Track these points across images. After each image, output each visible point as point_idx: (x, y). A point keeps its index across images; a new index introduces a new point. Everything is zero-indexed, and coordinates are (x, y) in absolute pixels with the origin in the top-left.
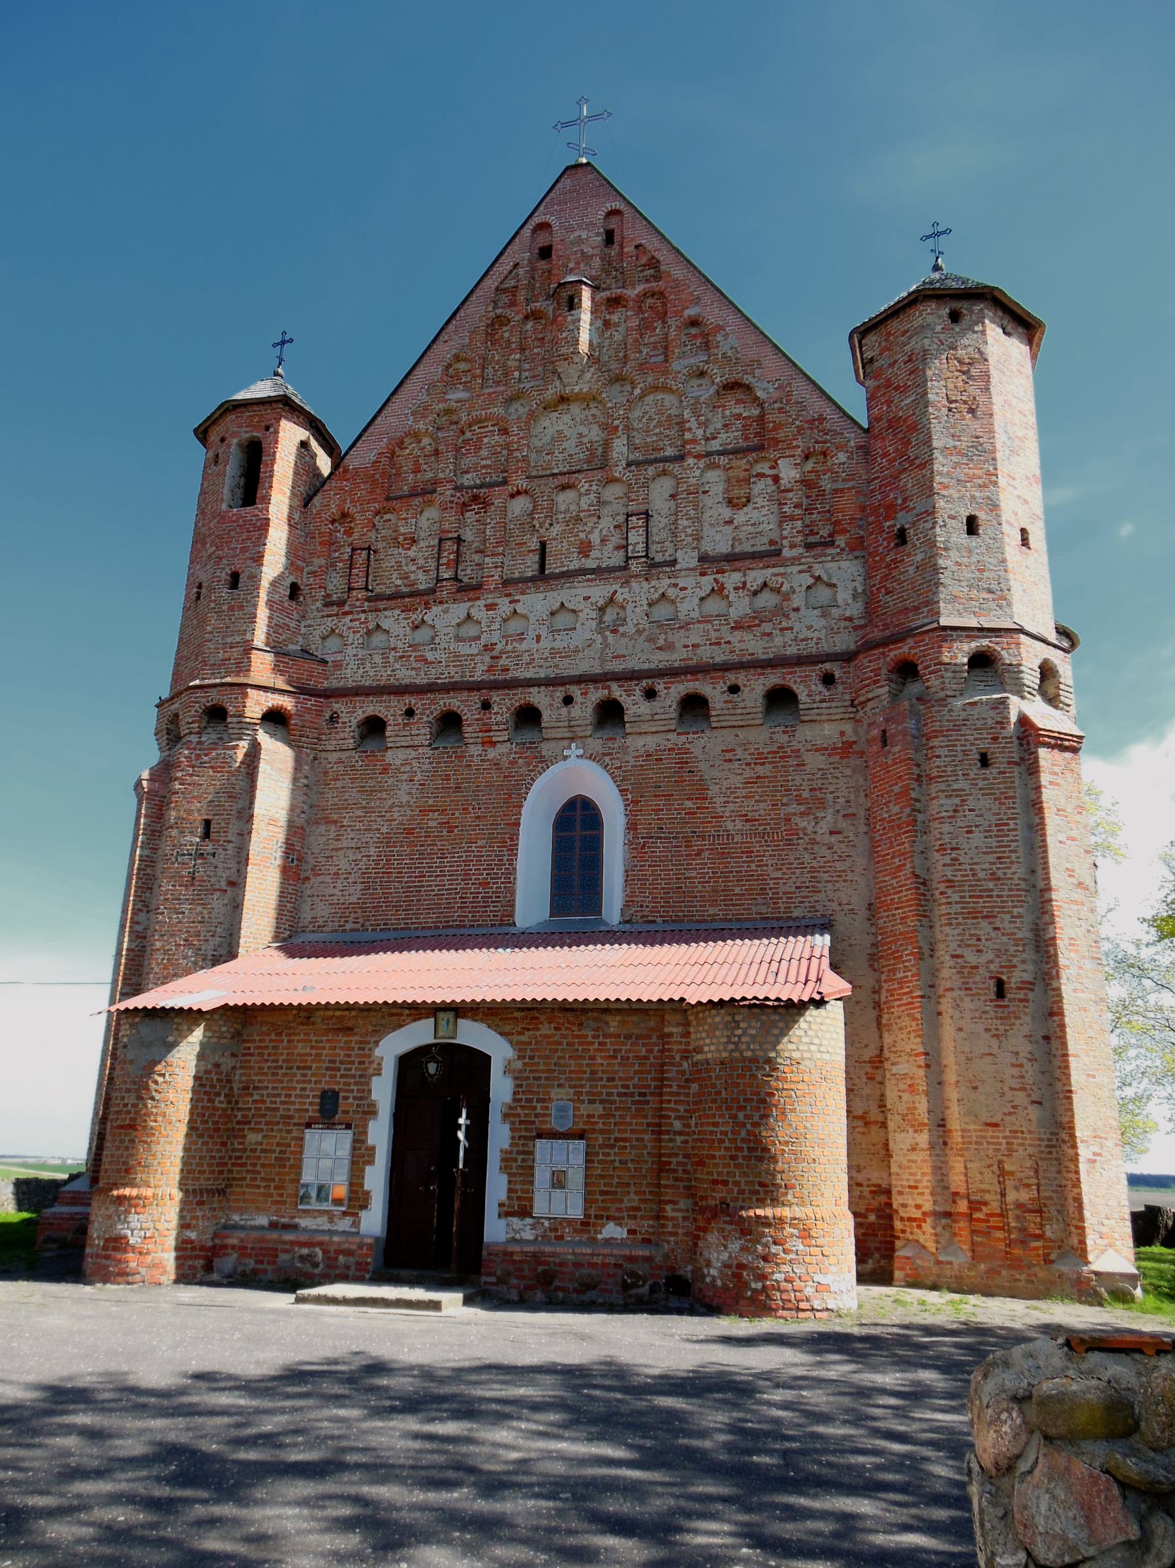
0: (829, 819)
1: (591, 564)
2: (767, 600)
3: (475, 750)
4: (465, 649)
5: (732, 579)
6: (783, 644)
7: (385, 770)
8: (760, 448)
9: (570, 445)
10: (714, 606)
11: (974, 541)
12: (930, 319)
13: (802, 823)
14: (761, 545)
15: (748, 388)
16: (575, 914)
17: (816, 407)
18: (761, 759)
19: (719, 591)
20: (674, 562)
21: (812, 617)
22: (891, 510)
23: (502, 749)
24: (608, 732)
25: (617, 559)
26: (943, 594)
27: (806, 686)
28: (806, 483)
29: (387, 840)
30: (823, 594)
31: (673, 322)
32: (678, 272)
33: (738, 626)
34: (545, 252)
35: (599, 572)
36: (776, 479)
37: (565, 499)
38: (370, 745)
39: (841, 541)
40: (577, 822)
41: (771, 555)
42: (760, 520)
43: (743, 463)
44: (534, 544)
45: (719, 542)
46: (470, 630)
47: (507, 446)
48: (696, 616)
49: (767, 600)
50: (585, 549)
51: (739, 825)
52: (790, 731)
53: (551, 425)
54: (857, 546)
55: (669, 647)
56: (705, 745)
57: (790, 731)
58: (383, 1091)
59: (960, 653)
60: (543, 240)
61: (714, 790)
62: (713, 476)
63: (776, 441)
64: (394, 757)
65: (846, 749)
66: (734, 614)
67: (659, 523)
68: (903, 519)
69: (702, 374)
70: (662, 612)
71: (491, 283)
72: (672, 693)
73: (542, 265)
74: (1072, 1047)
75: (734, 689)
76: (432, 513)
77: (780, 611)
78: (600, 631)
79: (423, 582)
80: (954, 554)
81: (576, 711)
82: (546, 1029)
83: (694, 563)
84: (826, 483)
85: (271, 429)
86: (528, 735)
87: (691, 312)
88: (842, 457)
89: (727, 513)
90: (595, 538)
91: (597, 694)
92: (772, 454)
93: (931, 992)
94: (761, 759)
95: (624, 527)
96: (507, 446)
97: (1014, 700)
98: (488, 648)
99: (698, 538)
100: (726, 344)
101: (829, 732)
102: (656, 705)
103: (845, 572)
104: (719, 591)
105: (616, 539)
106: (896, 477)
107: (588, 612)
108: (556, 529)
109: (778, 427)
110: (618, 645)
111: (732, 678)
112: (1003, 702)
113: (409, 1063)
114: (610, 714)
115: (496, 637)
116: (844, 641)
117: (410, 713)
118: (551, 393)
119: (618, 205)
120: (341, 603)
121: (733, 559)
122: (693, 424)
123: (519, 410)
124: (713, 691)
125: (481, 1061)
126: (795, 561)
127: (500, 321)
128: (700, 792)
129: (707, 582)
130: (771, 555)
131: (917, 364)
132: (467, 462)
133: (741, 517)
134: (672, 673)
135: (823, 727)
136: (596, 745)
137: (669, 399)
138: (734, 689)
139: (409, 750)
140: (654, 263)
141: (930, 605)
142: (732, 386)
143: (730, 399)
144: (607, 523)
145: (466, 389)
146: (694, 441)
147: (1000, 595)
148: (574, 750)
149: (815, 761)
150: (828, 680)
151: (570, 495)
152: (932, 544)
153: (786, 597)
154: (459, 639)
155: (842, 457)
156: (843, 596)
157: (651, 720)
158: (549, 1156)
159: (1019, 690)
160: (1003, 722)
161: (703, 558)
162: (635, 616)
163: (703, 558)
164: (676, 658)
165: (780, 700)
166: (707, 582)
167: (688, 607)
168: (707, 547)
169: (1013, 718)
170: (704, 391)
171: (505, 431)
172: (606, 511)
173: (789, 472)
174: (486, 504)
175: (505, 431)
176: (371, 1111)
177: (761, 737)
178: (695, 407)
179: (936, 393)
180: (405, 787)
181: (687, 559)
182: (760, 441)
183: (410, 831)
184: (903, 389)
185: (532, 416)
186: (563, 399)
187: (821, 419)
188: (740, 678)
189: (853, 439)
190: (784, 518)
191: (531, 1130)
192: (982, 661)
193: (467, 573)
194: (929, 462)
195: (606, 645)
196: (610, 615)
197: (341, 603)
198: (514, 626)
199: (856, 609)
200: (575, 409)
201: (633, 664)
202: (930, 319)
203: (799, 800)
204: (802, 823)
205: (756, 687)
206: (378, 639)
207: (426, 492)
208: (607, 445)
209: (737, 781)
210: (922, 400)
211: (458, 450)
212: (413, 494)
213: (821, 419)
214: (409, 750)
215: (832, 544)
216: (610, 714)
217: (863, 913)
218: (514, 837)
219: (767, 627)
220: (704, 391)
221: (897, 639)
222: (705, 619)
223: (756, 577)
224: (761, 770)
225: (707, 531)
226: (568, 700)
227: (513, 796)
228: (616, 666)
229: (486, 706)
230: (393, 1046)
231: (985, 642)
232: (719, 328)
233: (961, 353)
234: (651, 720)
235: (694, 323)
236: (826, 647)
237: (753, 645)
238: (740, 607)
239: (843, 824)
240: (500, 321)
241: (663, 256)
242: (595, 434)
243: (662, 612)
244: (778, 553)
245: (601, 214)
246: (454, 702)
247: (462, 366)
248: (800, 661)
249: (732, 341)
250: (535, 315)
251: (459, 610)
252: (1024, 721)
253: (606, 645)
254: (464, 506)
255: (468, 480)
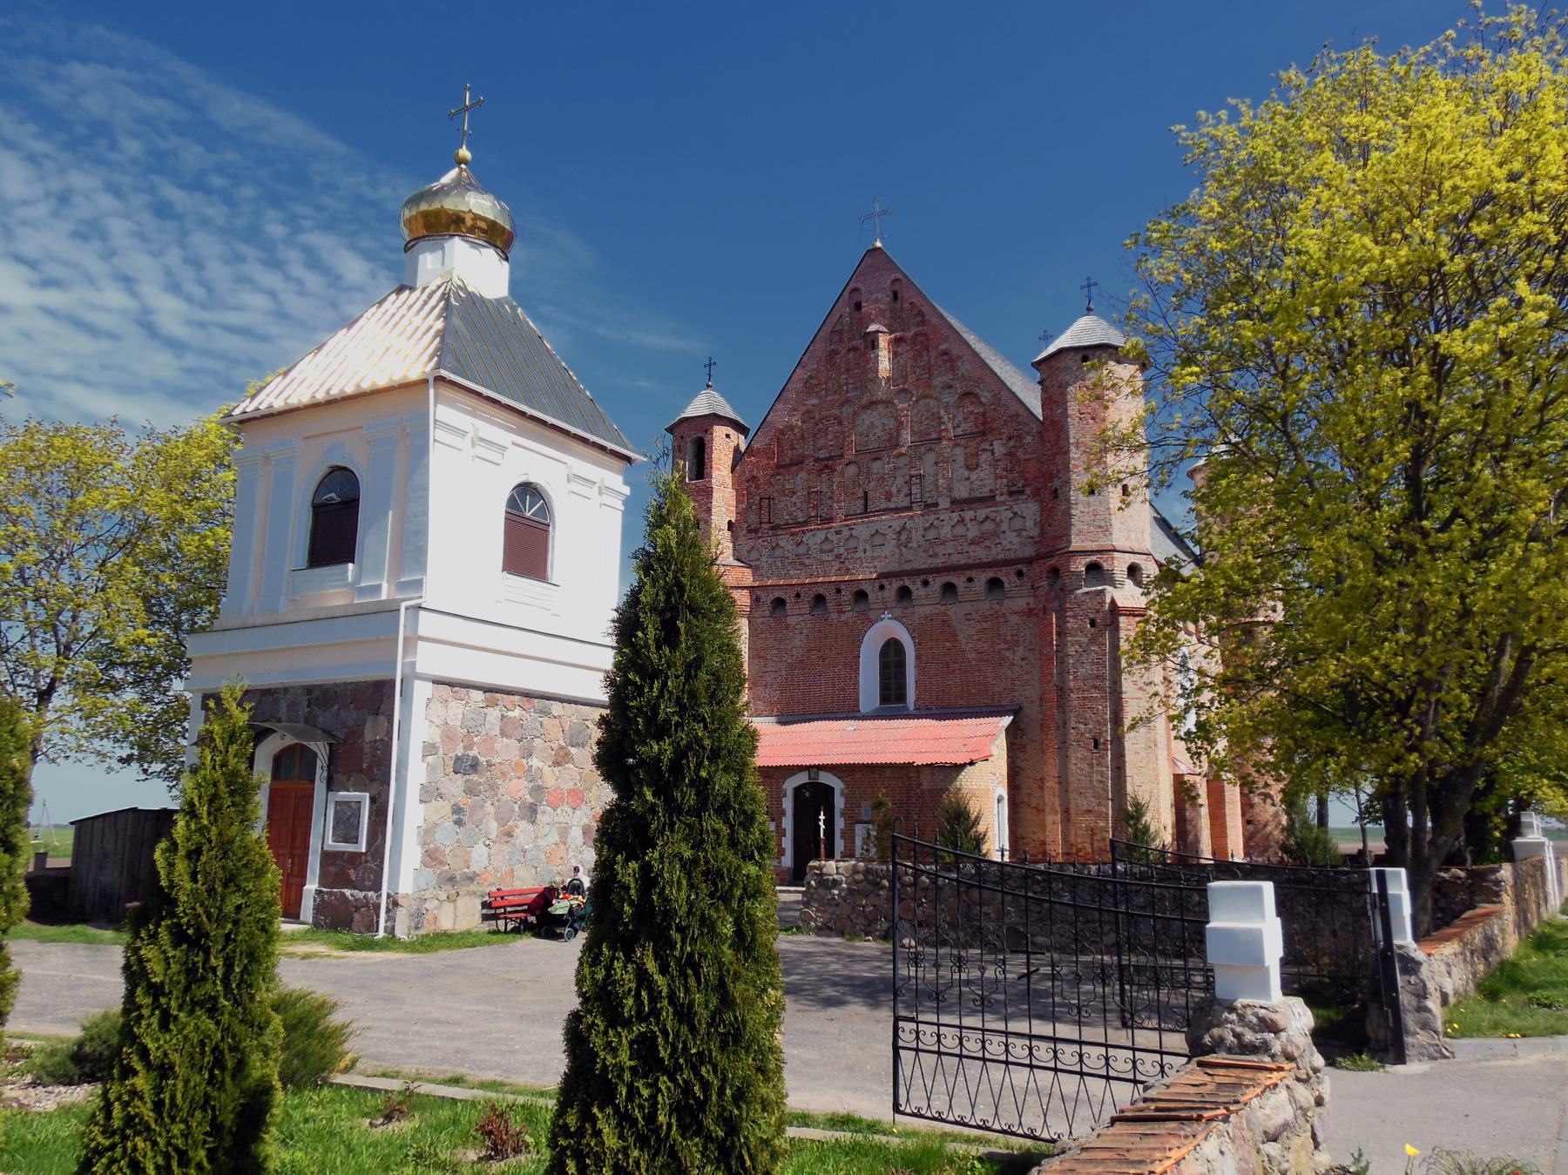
0: (1020, 652)
1: (892, 506)
2: (988, 526)
3: (834, 616)
4: (825, 557)
5: (969, 514)
6: (997, 553)
7: (787, 628)
8: (984, 433)
9: (879, 431)
10: (960, 530)
11: (1092, 498)
12: (1070, 363)
13: (1007, 654)
14: (985, 492)
15: (977, 396)
16: (892, 702)
17: (1014, 408)
18: (985, 618)
19: (962, 521)
20: (936, 505)
21: (1012, 536)
22: (1051, 476)
23: (849, 615)
24: (905, 604)
25: (906, 503)
26: (1074, 530)
27: (1008, 577)
28: (1010, 454)
29: (790, 666)
30: (1018, 523)
31: (933, 354)
32: (934, 320)
33: (972, 543)
34: (858, 306)
35: (896, 510)
36: (993, 452)
37: (876, 466)
38: (779, 613)
39: (1028, 491)
40: (892, 653)
41: (989, 500)
42: (985, 479)
43: (973, 444)
44: (861, 494)
45: (962, 492)
46: (827, 546)
47: (842, 433)
48: (953, 535)
49: (988, 526)
50: (889, 496)
51: (974, 655)
52: (1000, 603)
53: (867, 418)
54: (1037, 493)
55: (935, 555)
56: (956, 611)
57: (1000, 603)
58: (788, 804)
59: (1080, 565)
60: (855, 299)
61: (961, 636)
62: (958, 450)
63: (992, 429)
64: (791, 621)
65: (1030, 613)
66: (971, 535)
67: (929, 480)
68: (1056, 483)
69: (950, 387)
70: (931, 535)
71: (828, 328)
72: (937, 582)
73: (856, 315)
74: (1128, 772)
75: (970, 580)
76: (803, 475)
77: (994, 534)
78: (898, 546)
79: (801, 518)
80: (1080, 507)
81: (886, 594)
82: (858, 775)
83: (948, 505)
84: (1021, 455)
85: (708, 431)
86: (861, 606)
87: (943, 347)
88: (1029, 439)
89: (966, 473)
90: (894, 489)
91: (897, 584)
92: (990, 437)
93: (1064, 746)
94: (985, 618)
95: (909, 483)
96: (842, 433)
97: (1109, 588)
98: (838, 556)
99: (950, 490)
100: (964, 368)
101: (1021, 603)
102: (928, 590)
103: (1030, 510)
104: (962, 521)
105: (905, 490)
106: (1054, 456)
107: (891, 535)
108: (872, 484)
109: (993, 420)
110: (908, 555)
111: (968, 574)
112: (1102, 591)
113: (798, 791)
114: (904, 593)
115: (842, 550)
116: (1029, 551)
117: (798, 595)
118: (865, 400)
119: (898, 275)
120: (756, 531)
121: (970, 502)
122: (946, 419)
123: (848, 410)
124: (959, 581)
125: (829, 790)
126: (1003, 503)
127: (834, 352)
128: (953, 637)
129: (955, 516)
130: (989, 500)
131: (1063, 387)
132: (820, 443)
133: (974, 476)
134: (937, 571)
135: (1018, 601)
136: (898, 612)
137: (933, 403)
138: (970, 580)
139: (798, 615)
140: (921, 314)
141: (1066, 536)
142: (967, 394)
143: (967, 402)
144: (900, 481)
145: (819, 397)
146: (946, 430)
147: (1106, 530)
148: (887, 615)
149: (1014, 619)
150: (1020, 574)
151: (878, 464)
152: (1068, 500)
153: (998, 525)
154: (823, 551)
155: (1029, 439)
156: (1029, 524)
157: (926, 598)
158: (860, 830)
159: (1113, 583)
160: (1102, 603)
161: (954, 502)
162: (916, 537)
163: (954, 502)
164: (938, 562)
165: (995, 584)
166: (955, 516)
167: (946, 532)
168: (956, 494)
169: (1108, 601)
170: (949, 398)
171: (840, 423)
172: (898, 473)
173: (999, 449)
174: (833, 470)
175: (840, 423)
176: (783, 813)
177: (985, 606)
178: (947, 406)
179: (1073, 409)
180: (798, 637)
181: (944, 503)
182: (984, 430)
183: (802, 662)
184: (1058, 404)
185: (855, 414)
186: (873, 403)
187: (1017, 415)
188: (973, 574)
189: (1035, 428)
190: (997, 477)
191: (852, 819)
192: (1094, 568)
193: (824, 511)
194: (1067, 452)
195: (901, 554)
196: (904, 537)
197: (756, 531)
198: (851, 544)
199: (1035, 532)
200: (880, 408)
201: (916, 566)
202: (1070, 363)
203: (1005, 641)
204: (1007, 654)
205: (981, 578)
206: (778, 552)
207: (798, 462)
208: (898, 431)
209: (973, 631)
210: (1065, 414)
211: (815, 435)
212: (791, 465)
213: (1017, 415)
214: (798, 615)
215: (1021, 492)
216: (904, 593)
217: (1037, 702)
218: (857, 664)
219: (987, 543)
220: (949, 398)
221: (1050, 555)
222: (955, 538)
223: (982, 513)
224: (985, 625)
225: (957, 485)
226: (882, 587)
227: (856, 641)
228: (907, 567)
229: (838, 591)
230: (790, 784)
231: (1094, 558)
232: (959, 357)
233: (1088, 383)
234: (926, 598)
235: (945, 353)
236: (1020, 555)
237: (980, 553)
238: (973, 532)
239: (1028, 654)
240: (834, 352)
241: (925, 310)
242: (892, 424)
243: (931, 535)
244: (993, 497)
245: (889, 282)
246: (822, 590)
247: (814, 381)
248: (1006, 563)
249: (967, 366)
250: (855, 349)
251: (821, 536)
252: (1113, 601)
253: (901, 554)
254: (820, 472)
255: (822, 454)
